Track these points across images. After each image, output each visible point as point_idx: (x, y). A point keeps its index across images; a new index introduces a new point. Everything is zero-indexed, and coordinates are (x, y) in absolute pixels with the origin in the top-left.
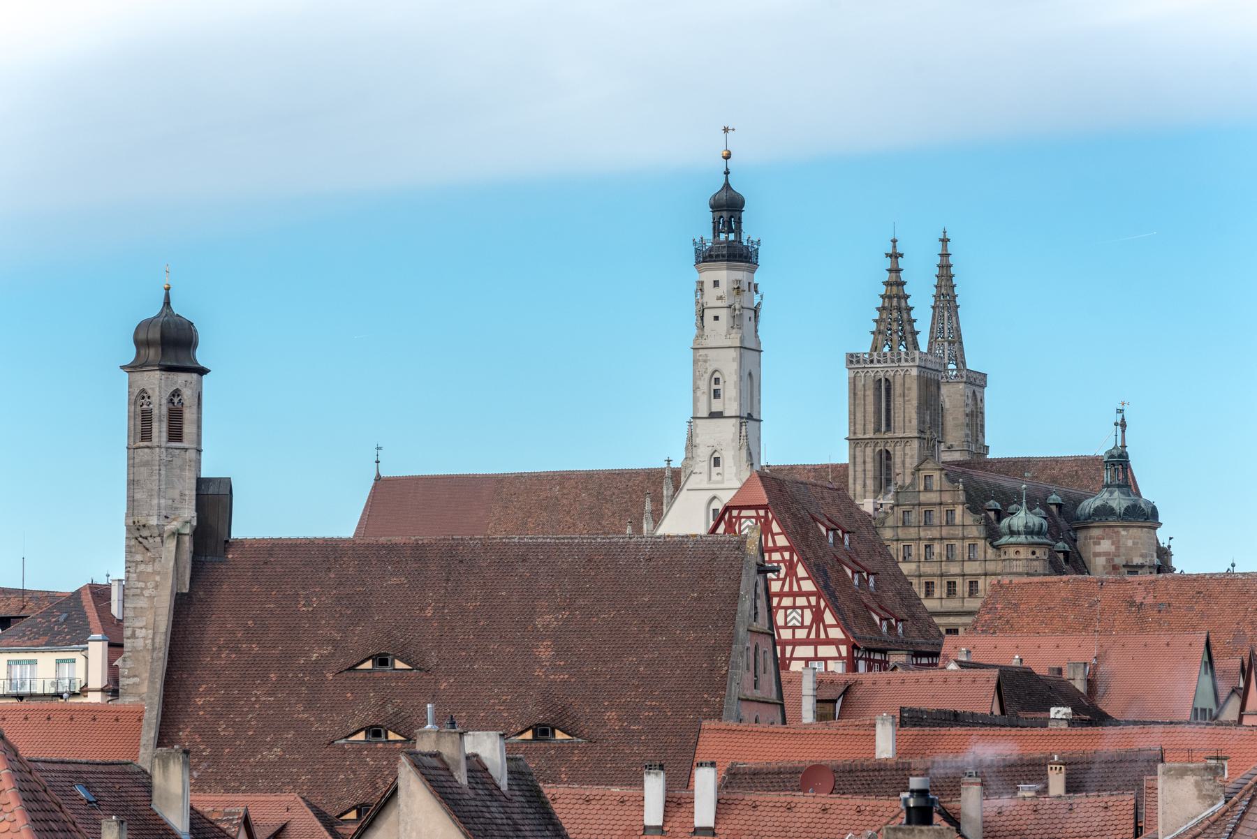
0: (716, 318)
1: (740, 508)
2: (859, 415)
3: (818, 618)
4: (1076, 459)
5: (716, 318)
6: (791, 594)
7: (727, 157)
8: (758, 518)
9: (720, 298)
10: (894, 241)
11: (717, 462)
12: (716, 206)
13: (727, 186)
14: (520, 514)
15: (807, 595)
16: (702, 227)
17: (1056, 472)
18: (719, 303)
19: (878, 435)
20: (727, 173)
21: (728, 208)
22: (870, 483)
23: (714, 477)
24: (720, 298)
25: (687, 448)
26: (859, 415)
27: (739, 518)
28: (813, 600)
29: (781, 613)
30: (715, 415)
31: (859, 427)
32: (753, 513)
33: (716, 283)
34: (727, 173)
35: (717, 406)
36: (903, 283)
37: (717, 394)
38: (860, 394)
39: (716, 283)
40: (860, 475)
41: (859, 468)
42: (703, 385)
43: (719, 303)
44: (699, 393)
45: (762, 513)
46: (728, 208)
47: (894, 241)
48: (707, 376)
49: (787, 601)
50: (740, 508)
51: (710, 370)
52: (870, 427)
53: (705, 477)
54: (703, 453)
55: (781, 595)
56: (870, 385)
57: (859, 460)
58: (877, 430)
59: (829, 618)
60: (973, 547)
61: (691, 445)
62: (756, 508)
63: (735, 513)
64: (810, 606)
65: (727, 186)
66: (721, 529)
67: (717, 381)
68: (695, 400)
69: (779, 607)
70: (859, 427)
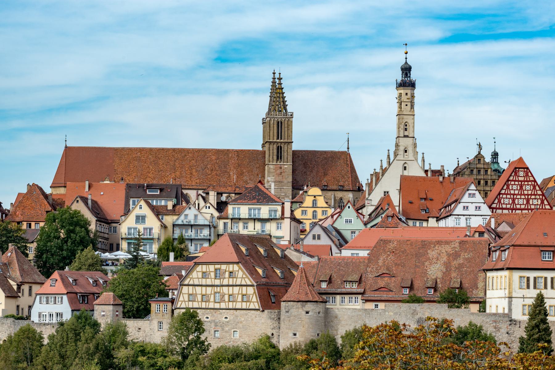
0: (406, 105)
1: (519, 168)
2: (271, 133)
3: (542, 202)
4: (332, 152)
5: (406, 105)
6: (534, 195)
7: (406, 53)
8: (524, 171)
9: (408, 99)
10: (280, 74)
11: (406, 151)
12: (402, 69)
13: (406, 63)
14: (126, 162)
15: (539, 195)
16: (399, 76)
17: (325, 156)
18: (408, 100)
19: (278, 141)
20: (406, 58)
21: (406, 70)
22: (275, 158)
23: (405, 156)
24: (408, 99)
25: (396, 146)
26: (271, 133)
27: (519, 171)
28: (541, 197)
29: (531, 200)
30: (405, 136)
31: (271, 138)
32: (523, 170)
33: (407, 94)
34: (406, 58)
35: (406, 133)
36: (283, 88)
37: (406, 130)
38: (272, 126)
39: (407, 94)
40: (271, 154)
41: (271, 152)
42: (402, 126)
43: (408, 100)
44: (400, 129)
45: (526, 170)
46: (406, 70)
47: (280, 74)
48: (403, 124)
49: (533, 197)
50: (519, 168)
51: (404, 122)
52: (275, 138)
53: (402, 156)
54: (402, 149)
55: (531, 195)
56: (276, 123)
57: (271, 149)
58: (278, 139)
59: (546, 202)
60: (494, 182)
61: (397, 145)
62: (524, 168)
63: (517, 170)
64: (540, 199)
65: (406, 63)
66: (513, 174)
67: (406, 125)
68: (399, 131)
69: (530, 198)
70: (271, 138)
